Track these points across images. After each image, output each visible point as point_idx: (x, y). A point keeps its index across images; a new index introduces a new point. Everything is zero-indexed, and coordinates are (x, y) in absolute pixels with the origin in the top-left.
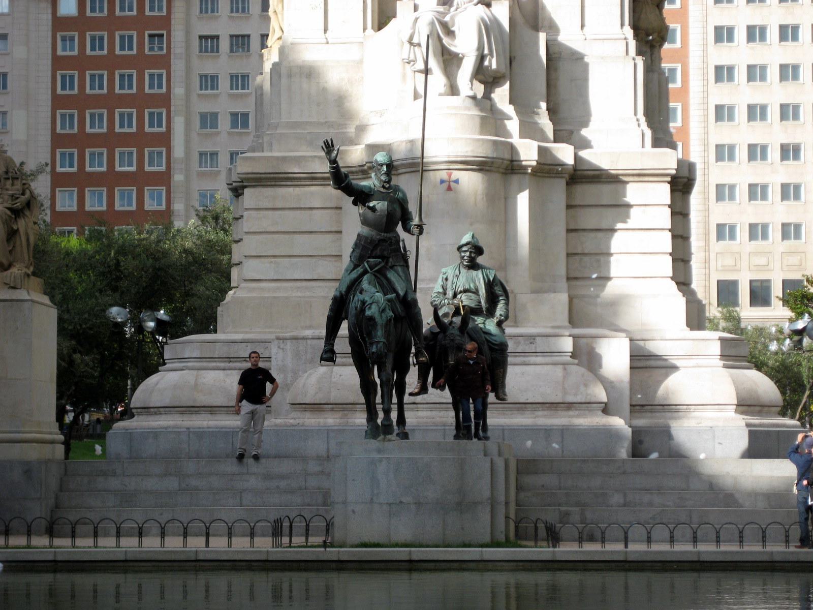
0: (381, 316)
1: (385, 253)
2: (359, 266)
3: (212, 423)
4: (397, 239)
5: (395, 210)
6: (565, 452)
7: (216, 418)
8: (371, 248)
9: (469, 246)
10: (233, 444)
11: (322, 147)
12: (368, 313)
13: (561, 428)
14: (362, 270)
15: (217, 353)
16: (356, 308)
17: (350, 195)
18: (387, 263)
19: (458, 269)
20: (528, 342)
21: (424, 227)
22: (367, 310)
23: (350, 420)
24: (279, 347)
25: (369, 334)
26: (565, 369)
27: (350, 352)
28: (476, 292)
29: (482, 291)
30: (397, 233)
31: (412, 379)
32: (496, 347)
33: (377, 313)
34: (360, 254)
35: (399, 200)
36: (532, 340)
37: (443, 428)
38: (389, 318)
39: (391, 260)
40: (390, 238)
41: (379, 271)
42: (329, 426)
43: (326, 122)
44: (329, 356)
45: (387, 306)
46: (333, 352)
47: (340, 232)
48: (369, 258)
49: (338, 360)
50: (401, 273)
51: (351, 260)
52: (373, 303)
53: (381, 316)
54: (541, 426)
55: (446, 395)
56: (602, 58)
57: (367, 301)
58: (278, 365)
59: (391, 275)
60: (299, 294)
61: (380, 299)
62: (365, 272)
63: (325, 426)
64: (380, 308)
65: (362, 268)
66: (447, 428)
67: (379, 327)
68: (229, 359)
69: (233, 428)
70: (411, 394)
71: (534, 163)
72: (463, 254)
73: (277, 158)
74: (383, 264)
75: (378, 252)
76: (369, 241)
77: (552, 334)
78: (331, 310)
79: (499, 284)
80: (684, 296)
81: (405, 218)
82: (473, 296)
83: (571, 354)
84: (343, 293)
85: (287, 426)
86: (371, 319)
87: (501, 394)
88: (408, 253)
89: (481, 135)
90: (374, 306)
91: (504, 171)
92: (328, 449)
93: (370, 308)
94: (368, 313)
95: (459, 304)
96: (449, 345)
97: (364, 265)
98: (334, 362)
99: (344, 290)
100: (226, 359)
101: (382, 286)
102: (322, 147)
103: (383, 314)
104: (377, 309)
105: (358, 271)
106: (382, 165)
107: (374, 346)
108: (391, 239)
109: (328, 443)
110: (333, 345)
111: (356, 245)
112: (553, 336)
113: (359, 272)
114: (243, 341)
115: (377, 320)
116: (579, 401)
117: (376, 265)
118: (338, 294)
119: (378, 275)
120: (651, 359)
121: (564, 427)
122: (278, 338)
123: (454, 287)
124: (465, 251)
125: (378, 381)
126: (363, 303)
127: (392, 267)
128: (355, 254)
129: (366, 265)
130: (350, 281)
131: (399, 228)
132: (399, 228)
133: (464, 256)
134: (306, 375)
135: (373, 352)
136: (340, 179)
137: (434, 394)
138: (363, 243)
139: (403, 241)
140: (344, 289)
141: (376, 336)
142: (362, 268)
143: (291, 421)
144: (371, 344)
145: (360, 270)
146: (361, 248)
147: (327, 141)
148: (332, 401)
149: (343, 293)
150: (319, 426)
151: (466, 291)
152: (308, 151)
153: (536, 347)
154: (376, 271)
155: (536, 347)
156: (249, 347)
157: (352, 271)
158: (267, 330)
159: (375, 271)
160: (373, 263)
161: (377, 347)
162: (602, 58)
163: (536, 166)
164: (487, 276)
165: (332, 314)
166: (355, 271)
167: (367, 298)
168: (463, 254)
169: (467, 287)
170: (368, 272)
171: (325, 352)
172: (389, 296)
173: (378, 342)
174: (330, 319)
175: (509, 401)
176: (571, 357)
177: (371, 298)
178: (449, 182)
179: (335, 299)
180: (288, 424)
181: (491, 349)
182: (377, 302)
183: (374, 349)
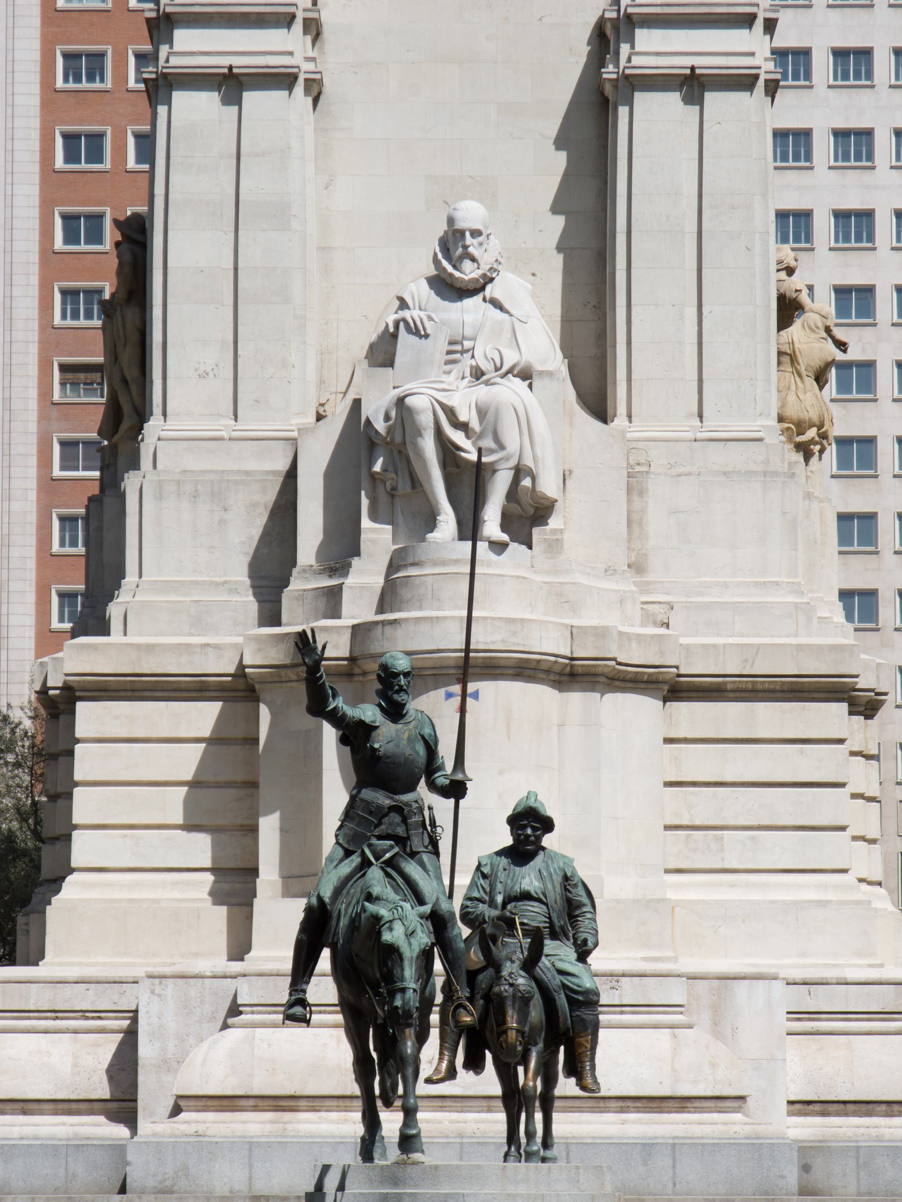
0: (410, 944)
1: (401, 831)
2: (353, 853)
3: (28, 1131)
5: (418, 753)
6: (677, 1186)
7: (721, 1128)
10: (66, 1169)
12: (387, 937)
13: (671, 1141)
15: (32, 1001)
18: (404, 847)
20: (608, 987)
21: (468, 784)
23: (289, 1127)
24: (152, 992)
26: (675, 1036)
27: (337, 1002)
31: (430, 1053)
32: (580, 998)
33: (403, 937)
35: (423, 737)
36: (614, 984)
37: (458, 1140)
41: (390, 863)
42: (252, 1137)
43: (226, 582)
44: (297, 1011)
45: (419, 926)
46: (303, 1003)
47: (253, 784)
49: (315, 1018)
51: (338, 843)
54: (634, 1138)
55: (488, 1081)
56: (725, 473)
57: (382, 917)
58: (150, 1025)
59: (412, 868)
60: (177, 895)
62: (365, 864)
63: (245, 1137)
64: (407, 929)
66: (465, 1140)
67: (406, 963)
68: (98, 1014)
69: (68, 1139)
70: (429, 1081)
73: (138, 647)
74: (396, 850)
77: (648, 972)
79: (580, 884)
81: (431, 765)
82: (536, 907)
85: (176, 1136)
87: (589, 1081)
88: (439, 830)
91: (557, 678)
92: (250, 1178)
93: (391, 929)
94: (387, 937)
95: (514, 919)
96: (506, 994)
97: (363, 853)
98: (308, 1022)
100: (49, 1014)
101: (397, 889)
103: (412, 940)
106: (396, 675)
108: (411, 806)
109: (251, 1166)
110: (304, 991)
112: (735, 979)
113: (354, 865)
114: (79, 980)
116: (702, 1093)
119: (389, 870)
121: (676, 1141)
122: (150, 977)
125: (374, 1055)
127: (413, 855)
128: (345, 830)
132: (422, 786)
134: (205, 1045)
135: (397, 1007)
137: (466, 1082)
139: (430, 808)
141: (402, 979)
143: (183, 1127)
145: (356, 860)
146: (357, 819)
148: (256, 1092)
149: (327, 900)
150: (234, 1137)
152: (192, 635)
153: (620, 997)
155: (620, 997)
156: (91, 992)
158: (118, 960)
159: (383, 863)
161: (403, 999)
162: (725, 473)
166: (347, 861)
167: (383, 912)
170: (371, 864)
171: (291, 1005)
174: (299, 946)
175: (603, 1093)
180: (176, 1132)
181: (570, 1000)
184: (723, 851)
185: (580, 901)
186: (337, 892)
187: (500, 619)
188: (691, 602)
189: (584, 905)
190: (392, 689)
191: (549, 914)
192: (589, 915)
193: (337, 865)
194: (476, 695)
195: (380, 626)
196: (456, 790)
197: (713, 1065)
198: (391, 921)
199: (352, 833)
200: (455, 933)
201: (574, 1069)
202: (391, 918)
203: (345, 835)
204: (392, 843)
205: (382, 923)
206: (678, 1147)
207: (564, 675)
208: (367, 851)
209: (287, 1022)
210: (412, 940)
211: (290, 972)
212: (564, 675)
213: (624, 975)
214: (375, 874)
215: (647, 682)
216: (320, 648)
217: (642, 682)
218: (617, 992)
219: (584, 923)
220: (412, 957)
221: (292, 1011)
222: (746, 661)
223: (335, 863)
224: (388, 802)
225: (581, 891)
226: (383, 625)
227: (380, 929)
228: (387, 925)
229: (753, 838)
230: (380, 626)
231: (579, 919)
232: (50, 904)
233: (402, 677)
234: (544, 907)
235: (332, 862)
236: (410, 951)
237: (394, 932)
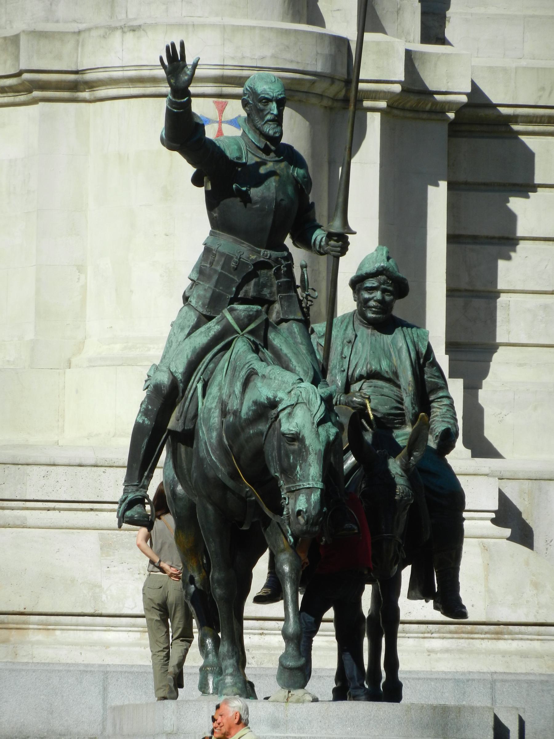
2: (210, 318)
8: (238, 280)
9: (382, 278)
13: (489, 677)
14: (218, 328)
16: (224, 413)
19: (350, 327)
21: (351, 238)
22: (283, 421)
25: (288, 471)
28: (393, 380)
29: (406, 377)
30: (286, 249)
33: (308, 426)
34: (214, 292)
38: (332, 438)
39: (277, 306)
48: (232, 301)
52: (297, 404)
53: (318, 434)
57: (281, 400)
65: (218, 323)
70: (259, 600)
71: (397, 88)
72: (366, 295)
74: (264, 317)
75: (250, 289)
76: (233, 265)
78: (145, 412)
83: (493, 515)
84: (179, 377)
86: (296, 438)
89: (283, 20)
90: (299, 412)
94: (287, 426)
103: (320, 429)
104: (308, 419)
105: (209, 328)
106: (268, 101)
111: (201, 272)
113: (212, 333)
115: (307, 442)
117: (251, 318)
118: (164, 378)
123: (346, 367)
124: (371, 289)
129: (229, 317)
130: (193, 351)
133: (369, 300)
135: (299, 513)
138: (219, 268)
140: (179, 368)
141: (305, 478)
142: (218, 323)
146: (215, 277)
147: (173, 45)
149: (179, 377)
151: (373, 375)
161: (308, 500)
163: (398, 94)
164: (415, 345)
166: (202, 329)
167: (281, 395)
168: (366, 295)
169: (375, 366)
176: (493, 521)
177: (290, 392)
178: (220, 122)
182: (308, 403)
183: (301, 504)
184: (509, 321)
185: (436, 384)
186: (192, 367)
187: (272, 29)
188: (472, 14)
190: (262, 118)
191: (402, 400)
192: (446, 401)
193: (189, 334)
195: (118, 33)
197: (536, 585)
198: (293, 406)
199: (208, 295)
201: (421, 589)
202: (293, 402)
203: (199, 297)
204: (260, 307)
205: (280, 407)
206: (498, 685)
207: (337, 100)
208: (229, 317)
209: (125, 525)
211: (126, 464)
212: (337, 100)
214: (240, 345)
215: (430, 112)
217: (424, 112)
221: (128, 513)
222: (543, 89)
223: (187, 331)
224: (253, 257)
226: (124, 32)
227: (278, 416)
229: (546, 307)
230: (118, 33)
234: (395, 389)
235: (182, 329)
236: (314, 443)
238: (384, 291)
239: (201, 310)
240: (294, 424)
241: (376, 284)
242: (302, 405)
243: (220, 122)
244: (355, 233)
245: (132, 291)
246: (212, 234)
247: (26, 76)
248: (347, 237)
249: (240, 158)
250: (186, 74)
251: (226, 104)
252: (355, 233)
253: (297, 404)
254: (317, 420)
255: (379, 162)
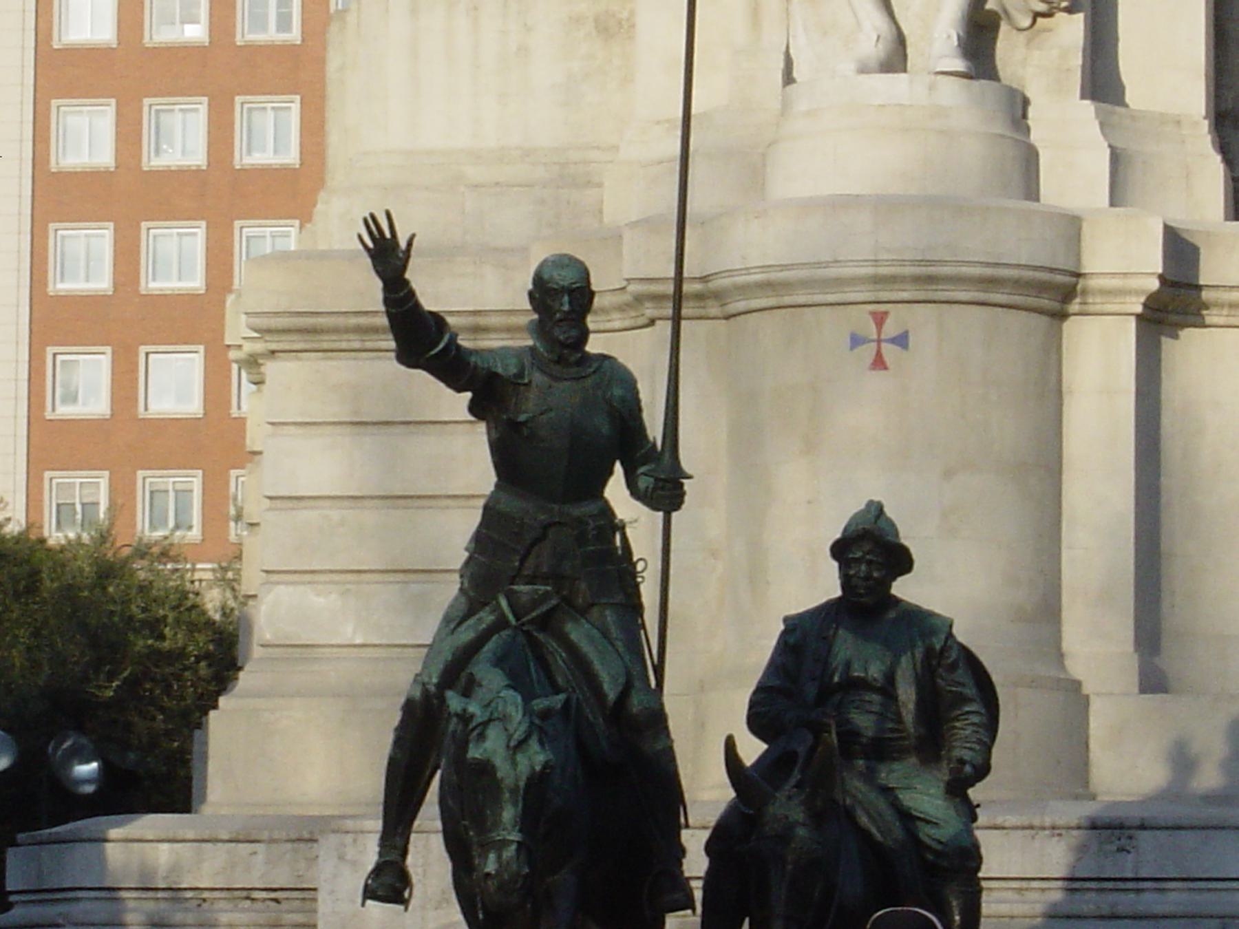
0: (514, 764)
4: (609, 524)
11: (360, 237)
14: (492, 618)
17: (457, 386)
24: (341, 858)
38: (538, 768)
40: (580, 521)
50: (614, 632)
52: (490, 720)
61: (511, 709)
64: (510, 737)
65: (492, 612)
77: (1185, 822)
78: (398, 742)
80: (215, 707)
84: (432, 689)
86: (485, 769)
93: (482, 737)
94: (474, 753)
99: (435, 680)
102: (360, 237)
103: (519, 757)
105: (480, 619)
107: (492, 856)
108: (588, 524)
115: (499, 775)
117: (535, 603)
118: (417, 694)
120: (78, 899)
124: (858, 561)
126: (465, 718)
129: (504, 603)
131: (616, 491)
132: (616, 491)
135: (488, 874)
136: (420, 337)
144: (486, 847)
145: (486, 617)
147: (373, 217)
149: (432, 689)
154: (531, 622)
156: (260, 857)
157: (459, 624)
160: (524, 599)
161: (499, 857)
163: (1158, 292)
165: (399, 756)
166: (471, 621)
171: (377, 871)
172: (539, 704)
173: (505, 843)
177: (488, 705)
178: (879, 341)
179: (409, 707)
189: (966, 700)
194: (901, 341)
196: (665, 493)
198: (485, 724)
200: (659, 746)
210: (519, 757)
213: (1142, 827)
216: (403, 244)
218: (1130, 857)
219: (965, 729)
220: (517, 786)
223: (452, 626)
225: (961, 674)
228: (475, 733)
231: (958, 724)
232: (215, 707)
233: (566, 298)
237: (488, 745)
238: (870, 563)
239: (472, 594)
240: (481, 751)
241: (859, 554)
242: (497, 723)
243: (879, 341)
244: (690, 477)
245: (768, 583)
246: (497, 486)
247: (632, 288)
248: (682, 485)
249: (520, 375)
250: (400, 259)
251: (886, 313)
252: (690, 477)
253: (490, 720)
254: (512, 744)
255: (1133, 389)
